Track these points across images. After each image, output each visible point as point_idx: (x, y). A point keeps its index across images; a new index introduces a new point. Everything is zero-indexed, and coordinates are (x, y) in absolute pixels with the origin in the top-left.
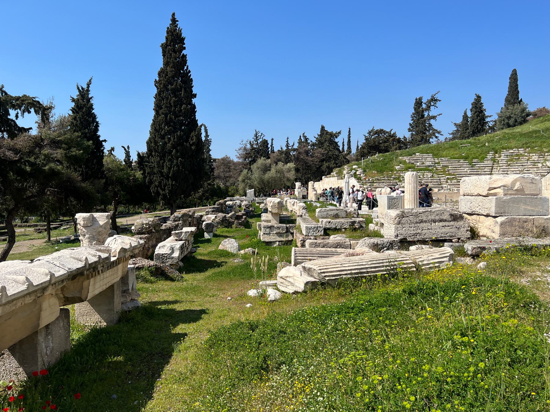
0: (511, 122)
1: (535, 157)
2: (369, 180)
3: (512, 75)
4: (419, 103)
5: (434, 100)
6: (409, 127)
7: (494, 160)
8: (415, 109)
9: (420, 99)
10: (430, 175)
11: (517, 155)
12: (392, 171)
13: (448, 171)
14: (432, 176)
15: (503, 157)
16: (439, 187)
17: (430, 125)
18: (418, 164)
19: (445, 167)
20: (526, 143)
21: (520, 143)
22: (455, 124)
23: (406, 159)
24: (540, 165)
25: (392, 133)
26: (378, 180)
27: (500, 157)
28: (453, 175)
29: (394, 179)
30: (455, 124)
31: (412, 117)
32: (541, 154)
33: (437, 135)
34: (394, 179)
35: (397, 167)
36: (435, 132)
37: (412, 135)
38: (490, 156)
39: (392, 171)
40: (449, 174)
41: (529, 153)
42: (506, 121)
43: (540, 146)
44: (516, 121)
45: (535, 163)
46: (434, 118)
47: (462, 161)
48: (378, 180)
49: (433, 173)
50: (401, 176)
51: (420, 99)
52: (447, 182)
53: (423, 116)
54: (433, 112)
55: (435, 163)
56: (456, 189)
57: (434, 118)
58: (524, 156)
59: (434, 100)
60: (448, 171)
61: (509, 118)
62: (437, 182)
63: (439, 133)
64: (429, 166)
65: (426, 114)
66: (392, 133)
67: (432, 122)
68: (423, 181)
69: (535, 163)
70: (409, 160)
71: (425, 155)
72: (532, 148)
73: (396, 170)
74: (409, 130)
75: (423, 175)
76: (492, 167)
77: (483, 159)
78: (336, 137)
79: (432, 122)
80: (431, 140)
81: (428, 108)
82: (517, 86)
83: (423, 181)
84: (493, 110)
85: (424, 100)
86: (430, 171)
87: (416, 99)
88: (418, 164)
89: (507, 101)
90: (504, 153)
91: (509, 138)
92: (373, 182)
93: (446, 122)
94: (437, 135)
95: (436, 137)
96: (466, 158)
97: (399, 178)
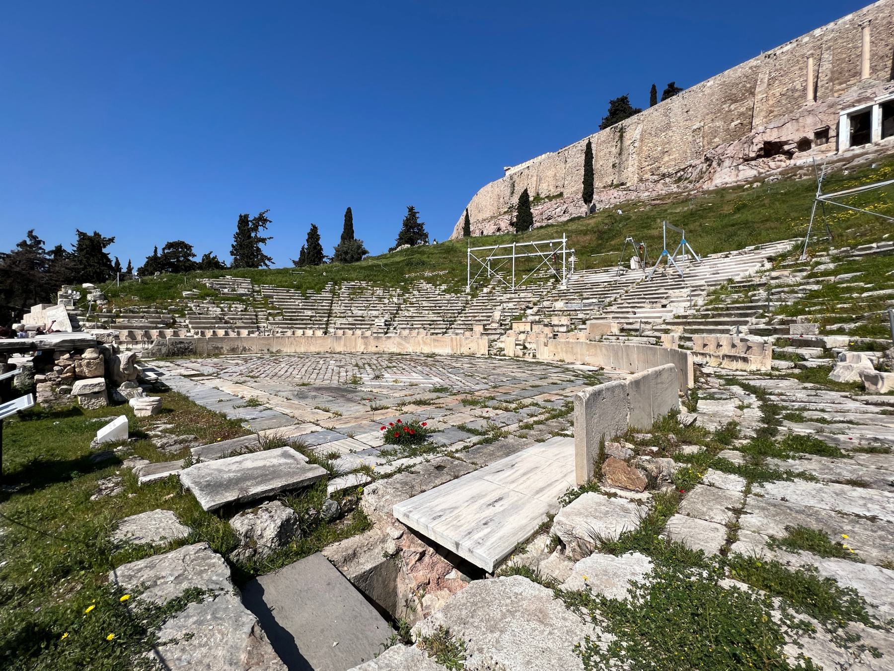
0: (348, 257)
1: (379, 292)
2: (110, 311)
3: (347, 213)
4: (243, 221)
5: (262, 220)
6: (231, 249)
7: (333, 292)
8: (239, 228)
9: (246, 216)
10: (241, 307)
11: (359, 288)
12: (173, 298)
13: (272, 303)
14: (246, 310)
15: (344, 289)
16: (253, 327)
17: (259, 250)
18: (226, 291)
19: (267, 297)
20: (368, 276)
21: (361, 276)
22: (294, 262)
23: (207, 282)
24: (386, 301)
25: (211, 256)
26: (133, 312)
27: (340, 289)
28: (279, 309)
29: (170, 311)
30: (294, 262)
31: (235, 237)
32: (385, 288)
33: (267, 262)
34: (170, 311)
35: (184, 293)
37: (236, 259)
38: (328, 287)
39: (173, 298)
40: (273, 308)
41: (372, 287)
42: (344, 256)
43: (383, 280)
44: (352, 257)
45: (380, 299)
46: (263, 240)
47: (292, 291)
48: (133, 312)
49: (247, 305)
50: (187, 307)
51: (246, 216)
52: (267, 319)
53: (250, 237)
54: (261, 233)
55: (254, 291)
56: (280, 330)
57: (263, 240)
58: (367, 289)
59: (262, 220)
60: (272, 303)
61: (346, 253)
62: (251, 319)
63: (269, 259)
64: (243, 295)
65: (253, 235)
66: (211, 256)
68: (226, 318)
69: (380, 299)
70: (212, 283)
71: (240, 280)
72: (375, 282)
73: (182, 297)
74: (232, 253)
75: (230, 307)
76: (332, 301)
77: (319, 291)
78: (105, 247)
81: (255, 229)
82: (351, 225)
83: (226, 318)
84: (330, 245)
86: (242, 301)
87: (241, 216)
88: (226, 291)
89: (343, 238)
90: (344, 286)
91: (349, 270)
92: (118, 316)
93: (282, 250)
94: (267, 262)
95: (266, 265)
96: (298, 288)
97: (183, 310)
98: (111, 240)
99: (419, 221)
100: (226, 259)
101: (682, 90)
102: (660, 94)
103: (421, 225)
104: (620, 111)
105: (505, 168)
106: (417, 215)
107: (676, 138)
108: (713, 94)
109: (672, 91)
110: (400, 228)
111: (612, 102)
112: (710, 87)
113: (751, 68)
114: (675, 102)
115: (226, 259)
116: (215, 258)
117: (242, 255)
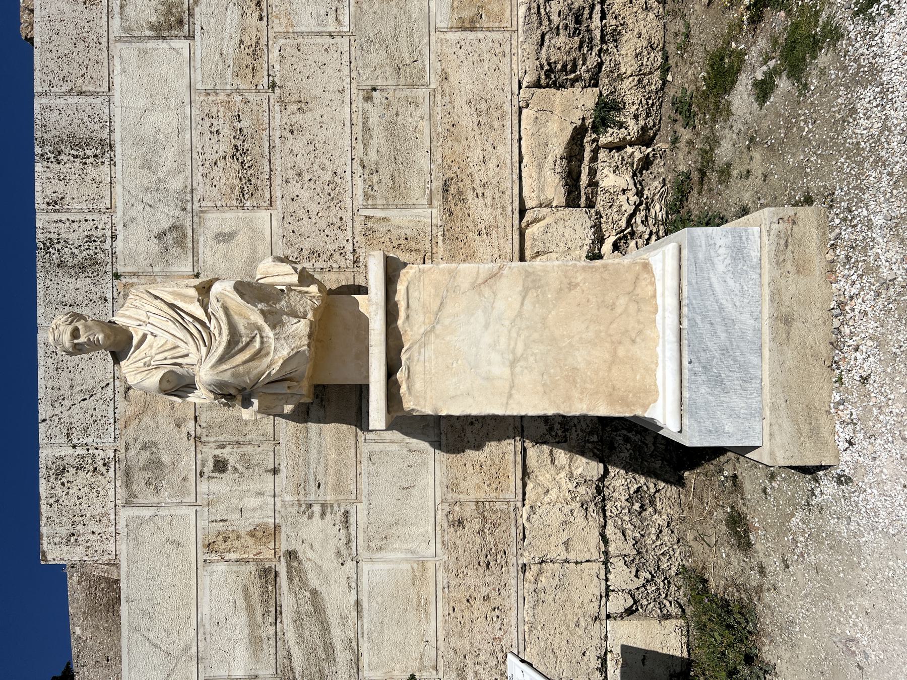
108: (97, 627)
112: (83, 630)
113: (79, 583)
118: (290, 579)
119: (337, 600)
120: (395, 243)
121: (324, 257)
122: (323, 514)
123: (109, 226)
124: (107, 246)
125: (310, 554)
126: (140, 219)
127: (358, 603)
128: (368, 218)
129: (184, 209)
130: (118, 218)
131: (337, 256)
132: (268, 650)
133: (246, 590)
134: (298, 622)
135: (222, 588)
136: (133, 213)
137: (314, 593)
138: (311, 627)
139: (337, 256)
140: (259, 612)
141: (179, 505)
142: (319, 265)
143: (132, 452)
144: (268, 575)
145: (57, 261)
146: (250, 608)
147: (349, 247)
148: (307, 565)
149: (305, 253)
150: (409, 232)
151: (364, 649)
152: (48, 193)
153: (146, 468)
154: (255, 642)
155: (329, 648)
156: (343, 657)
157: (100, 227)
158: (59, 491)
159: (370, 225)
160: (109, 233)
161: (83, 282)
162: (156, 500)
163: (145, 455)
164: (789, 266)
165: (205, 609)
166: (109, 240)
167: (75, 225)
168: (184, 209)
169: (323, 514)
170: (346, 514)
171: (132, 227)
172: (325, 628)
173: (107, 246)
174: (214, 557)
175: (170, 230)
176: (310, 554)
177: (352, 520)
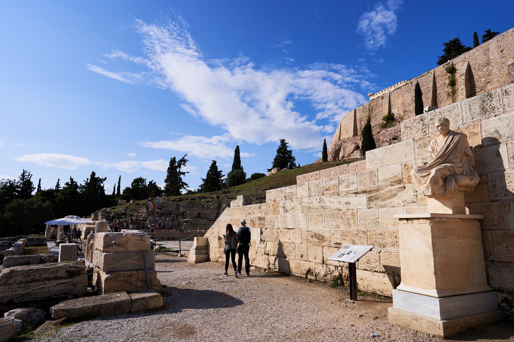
5: (183, 161)
9: (174, 158)
17: (181, 179)
22: (203, 180)
25: (153, 182)
30: (203, 180)
33: (185, 186)
36: (184, 185)
46: (184, 174)
54: (183, 169)
59: (183, 161)
63: (186, 185)
65: (178, 170)
66: (153, 182)
67: (182, 176)
79: (182, 176)
80: (181, 190)
81: (179, 166)
85: (177, 160)
94: (185, 186)
98: (105, 179)
99: (288, 149)
100: (162, 185)
101: (498, 33)
102: (480, 39)
103: (290, 152)
104: (455, 49)
105: (369, 95)
106: (287, 145)
107: (495, 71)
109: (490, 35)
110: (275, 154)
111: (446, 44)
114: (493, 43)
115: (162, 185)
116: (155, 183)
117: (172, 183)
118: (399, 188)
119: (395, 201)
120: (501, 215)
121: (494, 189)
122: (414, 195)
123: (499, 113)
124: (492, 114)
125: (405, 193)
126: (502, 123)
127: (394, 206)
128: (510, 205)
129: (508, 137)
130: (503, 115)
131: (494, 194)
132: (384, 184)
133: (396, 176)
134: (390, 191)
135: (396, 170)
136: (504, 120)
137: (396, 195)
138: (389, 194)
139: (494, 194)
140: (392, 180)
141: (415, 154)
142: (490, 188)
143: (428, 138)
144: (400, 181)
145: (485, 100)
146: (392, 178)
147: (498, 198)
148: (402, 192)
149: (494, 183)
150: (506, 220)
151: (385, 209)
152: (510, 89)
153: (424, 143)
154: (386, 180)
155: (384, 200)
156: (383, 203)
157: (499, 110)
158: (417, 121)
159: (507, 205)
160: (496, 114)
161: (478, 110)
162: (416, 148)
163: (427, 142)
164: (428, 324)
165: (392, 166)
166: (494, 114)
167: (499, 102)
168: (508, 137)
169: (414, 195)
170: (415, 202)
171: (499, 121)
172: (389, 198)
173: (492, 114)
174: (403, 166)
175: (499, 134)
176: (405, 193)
177: (414, 204)
